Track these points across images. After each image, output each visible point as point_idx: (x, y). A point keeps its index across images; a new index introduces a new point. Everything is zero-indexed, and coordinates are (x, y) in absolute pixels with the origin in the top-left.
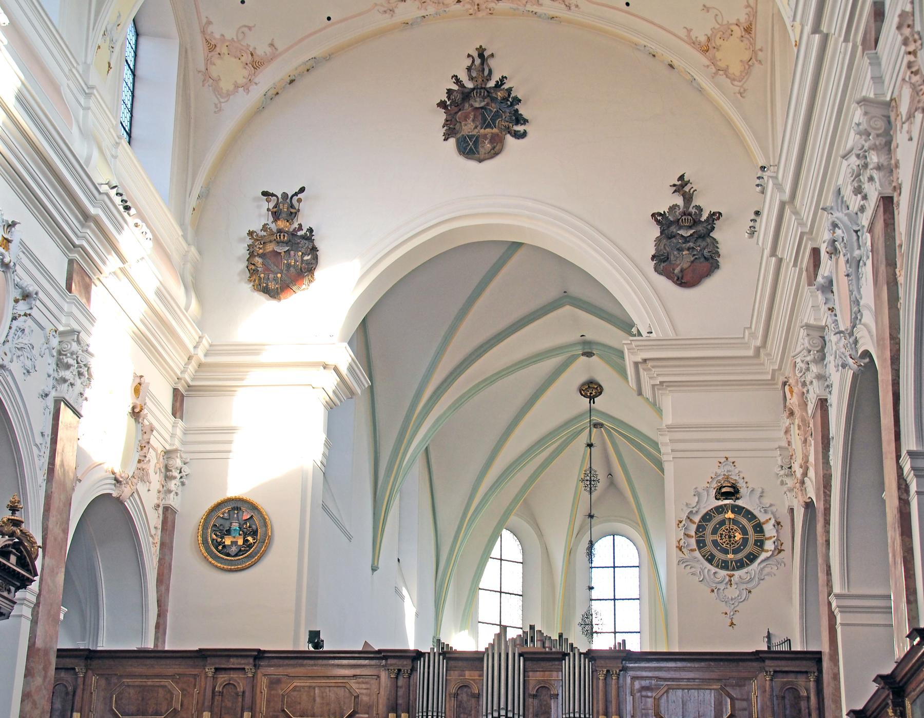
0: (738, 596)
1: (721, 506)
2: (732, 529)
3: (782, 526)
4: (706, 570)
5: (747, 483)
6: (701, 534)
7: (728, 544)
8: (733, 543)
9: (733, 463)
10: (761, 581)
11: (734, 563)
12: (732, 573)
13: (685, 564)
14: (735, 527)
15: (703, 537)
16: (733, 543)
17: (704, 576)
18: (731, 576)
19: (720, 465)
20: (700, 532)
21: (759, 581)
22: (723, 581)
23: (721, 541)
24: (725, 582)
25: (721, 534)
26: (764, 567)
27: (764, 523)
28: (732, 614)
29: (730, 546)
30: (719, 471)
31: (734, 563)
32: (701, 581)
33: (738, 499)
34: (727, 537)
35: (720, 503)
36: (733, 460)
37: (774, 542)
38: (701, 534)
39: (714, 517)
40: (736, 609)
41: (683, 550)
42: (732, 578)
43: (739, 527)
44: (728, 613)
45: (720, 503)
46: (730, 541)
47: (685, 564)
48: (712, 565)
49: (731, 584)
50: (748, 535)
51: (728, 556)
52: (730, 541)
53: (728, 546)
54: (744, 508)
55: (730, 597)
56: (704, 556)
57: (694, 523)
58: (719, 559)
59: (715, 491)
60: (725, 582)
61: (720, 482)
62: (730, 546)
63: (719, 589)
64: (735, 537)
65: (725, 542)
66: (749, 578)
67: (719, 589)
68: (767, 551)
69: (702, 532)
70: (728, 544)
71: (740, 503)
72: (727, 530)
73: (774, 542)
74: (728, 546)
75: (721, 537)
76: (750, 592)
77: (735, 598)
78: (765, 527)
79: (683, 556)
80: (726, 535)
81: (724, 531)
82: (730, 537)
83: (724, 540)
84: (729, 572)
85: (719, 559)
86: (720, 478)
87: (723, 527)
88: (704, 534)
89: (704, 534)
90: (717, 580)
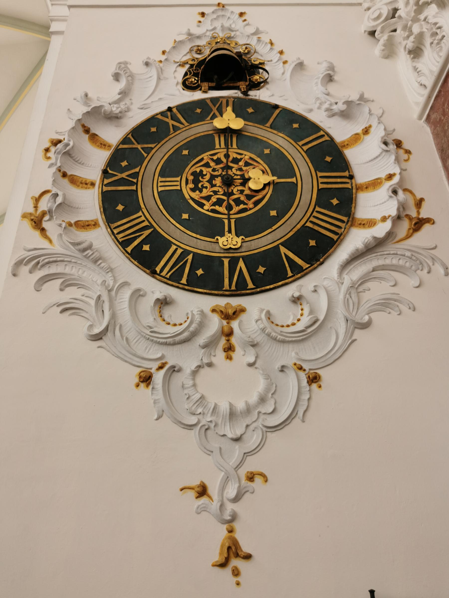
0: (262, 400)
1: (201, 103)
2: (236, 161)
3: (408, 152)
4: (126, 294)
5: (281, 52)
6: (124, 175)
7: (219, 202)
8: (238, 202)
9: (241, 14)
10: (358, 333)
11: (241, 264)
12: (235, 302)
14: (247, 155)
15: (132, 184)
16: (238, 202)
17: (113, 316)
19: (202, 19)
20: (123, 170)
21: (350, 334)
22: (194, 334)
23: (196, 195)
24: (202, 339)
25: (197, 176)
26: (364, 280)
27: (347, 144)
28: (231, 492)
29: (229, 208)
30: (197, 31)
31: (241, 264)
32: (98, 337)
33: (257, 86)
34: (218, 181)
35: (198, 95)
36: (242, 9)
37: (395, 192)
38: (124, 175)
39: (175, 129)
41: (45, 225)
42: (235, 324)
43: (261, 155)
44: (213, 490)
45: (198, 95)
46: (229, 194)
48: (153, 273)
49: (229, 349)
50: (294, 175)
51: (222, 240)
52: (229, 194)
53: (222, 209)
54: (276, 107)
55: (224, 407)
56: (124, 244)
57: (104, 145)
58: (185, 253)
59: (183, 70)
60: (202, 339)
61: (199, 51)
62: (229, 208)
63: (174, 370)
64: (245, 181)
65: (208, 198)
66: (306, 320)
67: (174, 370)
68: (371, 223)
70: (219, 202)
72: (218, 161)
73: (395, 192)
74: (222, 209)
75: (196, 181)
77: (248, 410)
78: (349, 154)
79: (44, 243)
80: (213, 177)
81: (207, 165)
83: (205, 193)
84: (222, 302)
85: (185, 253)
86: (202, 42)
87: (206, 156)
88: (135, 175)
89: (135, 175)
90: (171, 330)
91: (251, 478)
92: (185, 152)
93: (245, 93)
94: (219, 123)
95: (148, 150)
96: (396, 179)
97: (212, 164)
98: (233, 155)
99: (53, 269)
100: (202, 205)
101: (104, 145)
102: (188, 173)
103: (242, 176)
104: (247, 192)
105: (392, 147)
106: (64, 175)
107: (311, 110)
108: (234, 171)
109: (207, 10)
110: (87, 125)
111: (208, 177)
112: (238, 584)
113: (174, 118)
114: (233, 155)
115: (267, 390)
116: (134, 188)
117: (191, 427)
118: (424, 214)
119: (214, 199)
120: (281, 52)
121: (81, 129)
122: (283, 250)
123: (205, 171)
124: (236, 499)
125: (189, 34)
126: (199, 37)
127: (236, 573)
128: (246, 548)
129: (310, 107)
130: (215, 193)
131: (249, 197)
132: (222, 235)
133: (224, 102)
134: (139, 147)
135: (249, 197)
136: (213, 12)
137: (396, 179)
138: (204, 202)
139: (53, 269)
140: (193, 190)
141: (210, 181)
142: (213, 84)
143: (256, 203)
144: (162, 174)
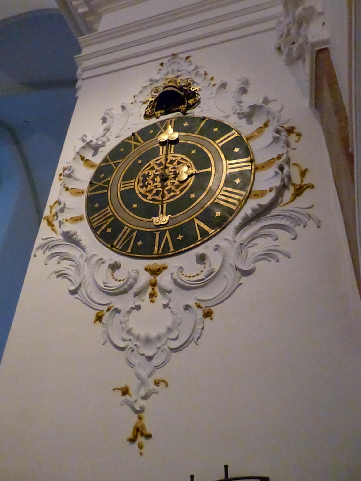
2: (172, 162)
6: (101, 184)
7: (157, 193)
8: (170, 191)
9: (187, 58)
12: (160, 262)
13: (48, 253)
18: (155, 272)
19: (161, 68)
22: (131, 287)
23: (142, 190)
29: (163, 196)
30: (156, 77)
31: (167, 235)
33: (190, 107)
34: (158, 179)
35: (153, 121)
37: (281, 168)
39: (136, 146)
40: (159, 375)
42: (158, 278)
44: (132, 391)
45: (153, 121)
46: (163, 187)
47: (48, 253)
48: (112, 247)
49: (152, 295)
53: (159, 198)
57: (92, 166)
63: (117, 311)
64: (176, 175)
65: (150, 191)
66: (205, 272)
69: (104, 178)
71: (196, 112)
75: (144, 181)
76: (208, 314)
77: (159, 338)
79: (53, 234)
80: (155, 176)
81: (153, 168)
82: (164, 179)
84: (150, 263)
85: (133, 231)
87: (152, 162)
90: (117, 284)
91: (157, 384)
92: (140, 162)
93: (184, 113)
94: (164, 137)
95: (116, 165)
96: (284, 158)
97: (156, 167)
98: (170, 158)
99: (56, 250)
100: (146, 197)
101: (92, 166)
102: (140, 177)
103: (175, 172)
104: (177, 183)
105: (284, 133)
106: (67, 189)
107: (228, 116)
108: (169, 171)
109: (164, 61)
110: (83, 155)
111: (151, 177)
112: (141, 454)
113: (136, 140)
114: (170, 158)
115: (174, 322)
116: (106, 191)
117: (122, 349)
118: (306, 181)
119: (154, 192)
120: (212, 79)
121: (79, 158)
122: (197, 221)
123: (152, 172)
124: (145, 398)
125: (151, 80)
126: (157, 81)
127: (141, 447)
128: (149, 430)
129: (227, 114)
130: (156, 187)
131: (177, 187)
132: (157, 216)
133: (169, 121)
134: (112, 163)
135: (177, 187)
136: (169, 61)
137: (284, 158)
138: (148, 194)
139: (56, 250)
140: (142, 187)
141: (153, 180)
142: (163, 112)
143: (181, 191)
144: (124, 180)
